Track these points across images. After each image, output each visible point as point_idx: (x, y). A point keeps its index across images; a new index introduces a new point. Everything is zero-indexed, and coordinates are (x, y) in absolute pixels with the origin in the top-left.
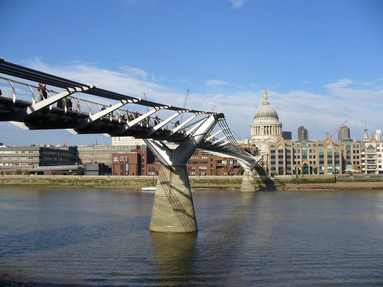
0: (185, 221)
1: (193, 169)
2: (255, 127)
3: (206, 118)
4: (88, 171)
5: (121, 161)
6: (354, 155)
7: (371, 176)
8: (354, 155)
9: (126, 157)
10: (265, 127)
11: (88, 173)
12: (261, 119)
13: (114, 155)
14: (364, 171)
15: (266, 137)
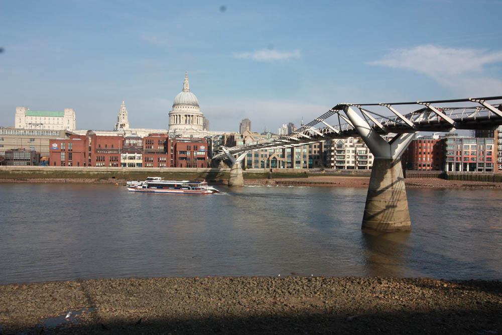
0: (388, 215)
1: (150, 159)
2: (174, 116)
3: (361, 111)
4: (14, 160)
5: (62, 148)
6: (315, 149)
7: (342, 171)
8: (315, 149)
9: (69, 144)
10: (186, 116)
11: (17, 162)
12: (182, 107)
13: (52, 141)
14: (333, 166)
15: (188, 127)
